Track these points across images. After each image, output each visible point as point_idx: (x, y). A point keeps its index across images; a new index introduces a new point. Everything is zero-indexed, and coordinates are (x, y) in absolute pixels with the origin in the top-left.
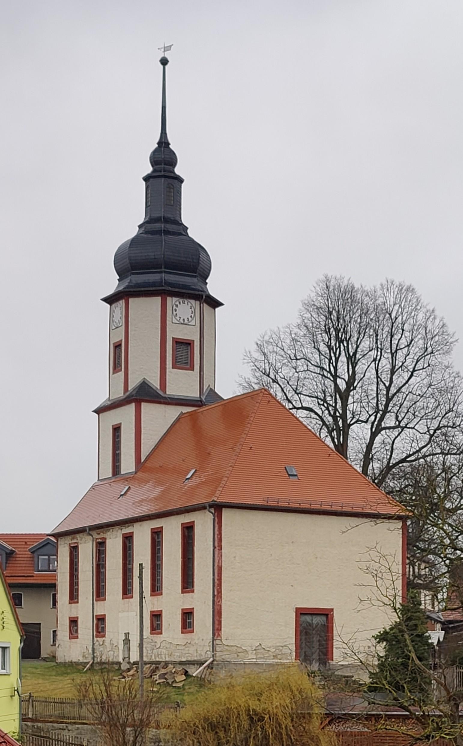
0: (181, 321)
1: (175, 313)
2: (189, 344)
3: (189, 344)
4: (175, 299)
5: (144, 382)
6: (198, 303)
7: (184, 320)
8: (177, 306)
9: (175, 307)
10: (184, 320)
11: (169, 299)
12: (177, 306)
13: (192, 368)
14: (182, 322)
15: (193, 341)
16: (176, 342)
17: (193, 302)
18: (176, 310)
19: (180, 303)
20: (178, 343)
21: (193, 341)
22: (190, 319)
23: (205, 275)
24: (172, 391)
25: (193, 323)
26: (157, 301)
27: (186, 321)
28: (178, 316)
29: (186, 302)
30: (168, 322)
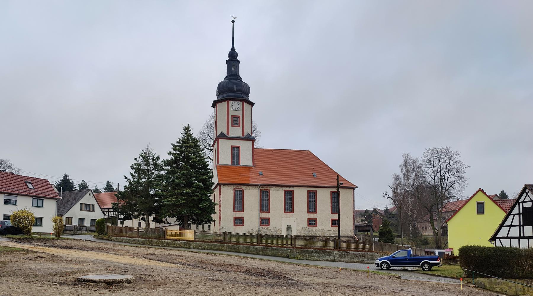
0: (235, 109)
1: (232, 107)
3: (238, 117)
4: (232, 102)
5: (221, 132)
6: (241, 103)
7: (236, 109)
8: (233, 104)
10: (236, 109)
12: (233, 104)
15: (240, 116)
16: (233, 117)
17: (239, 102)
20: (233, 117)
21: (240, 116)
23: (247, 94)
24: (231, 134)
26: (226, 103)
27: (237, 109)
29: (237, 102)
30: (230, 110)
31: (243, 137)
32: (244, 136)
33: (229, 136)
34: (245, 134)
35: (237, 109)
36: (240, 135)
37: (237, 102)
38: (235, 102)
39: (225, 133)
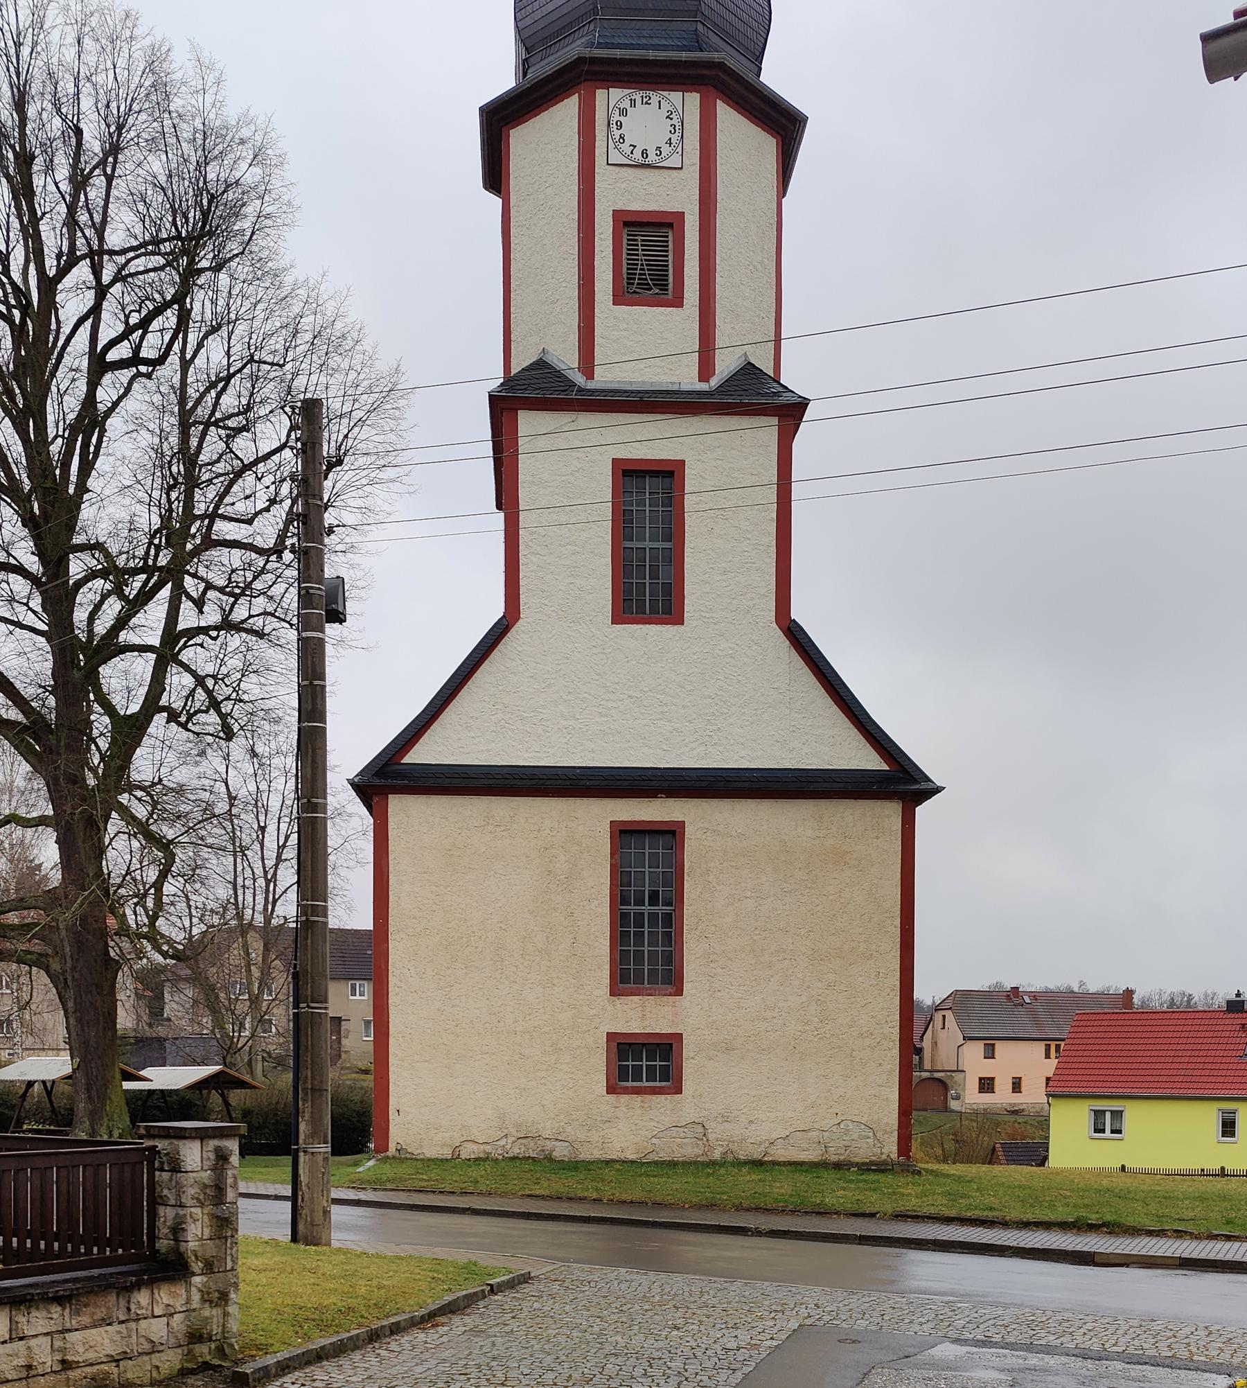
0: (637, 155)
1: (617, 134)
2: (670, 225)
4: (616, 94)
6: (693, 100)
7: (644, 153)
8: (623, 112)
9: (616, 117)
10: (644, 153)
11: (600, 94)
13: (678, 302)
14: (641, 160)
16: (626, 224)
17: (676, 97)
18: (620, 126)
19: (633, 103)
20: (628, 223)
22: (666, 150)
25: (675, 161)
28: (627, 143)
31: (704, 387)
32: (714, 382)
33: (591, 385)
34: (726, 364)
35: (652, 158)
36: (685, 376)
37: (655, 97)
38: (637, 96)
39: (566, 358)
